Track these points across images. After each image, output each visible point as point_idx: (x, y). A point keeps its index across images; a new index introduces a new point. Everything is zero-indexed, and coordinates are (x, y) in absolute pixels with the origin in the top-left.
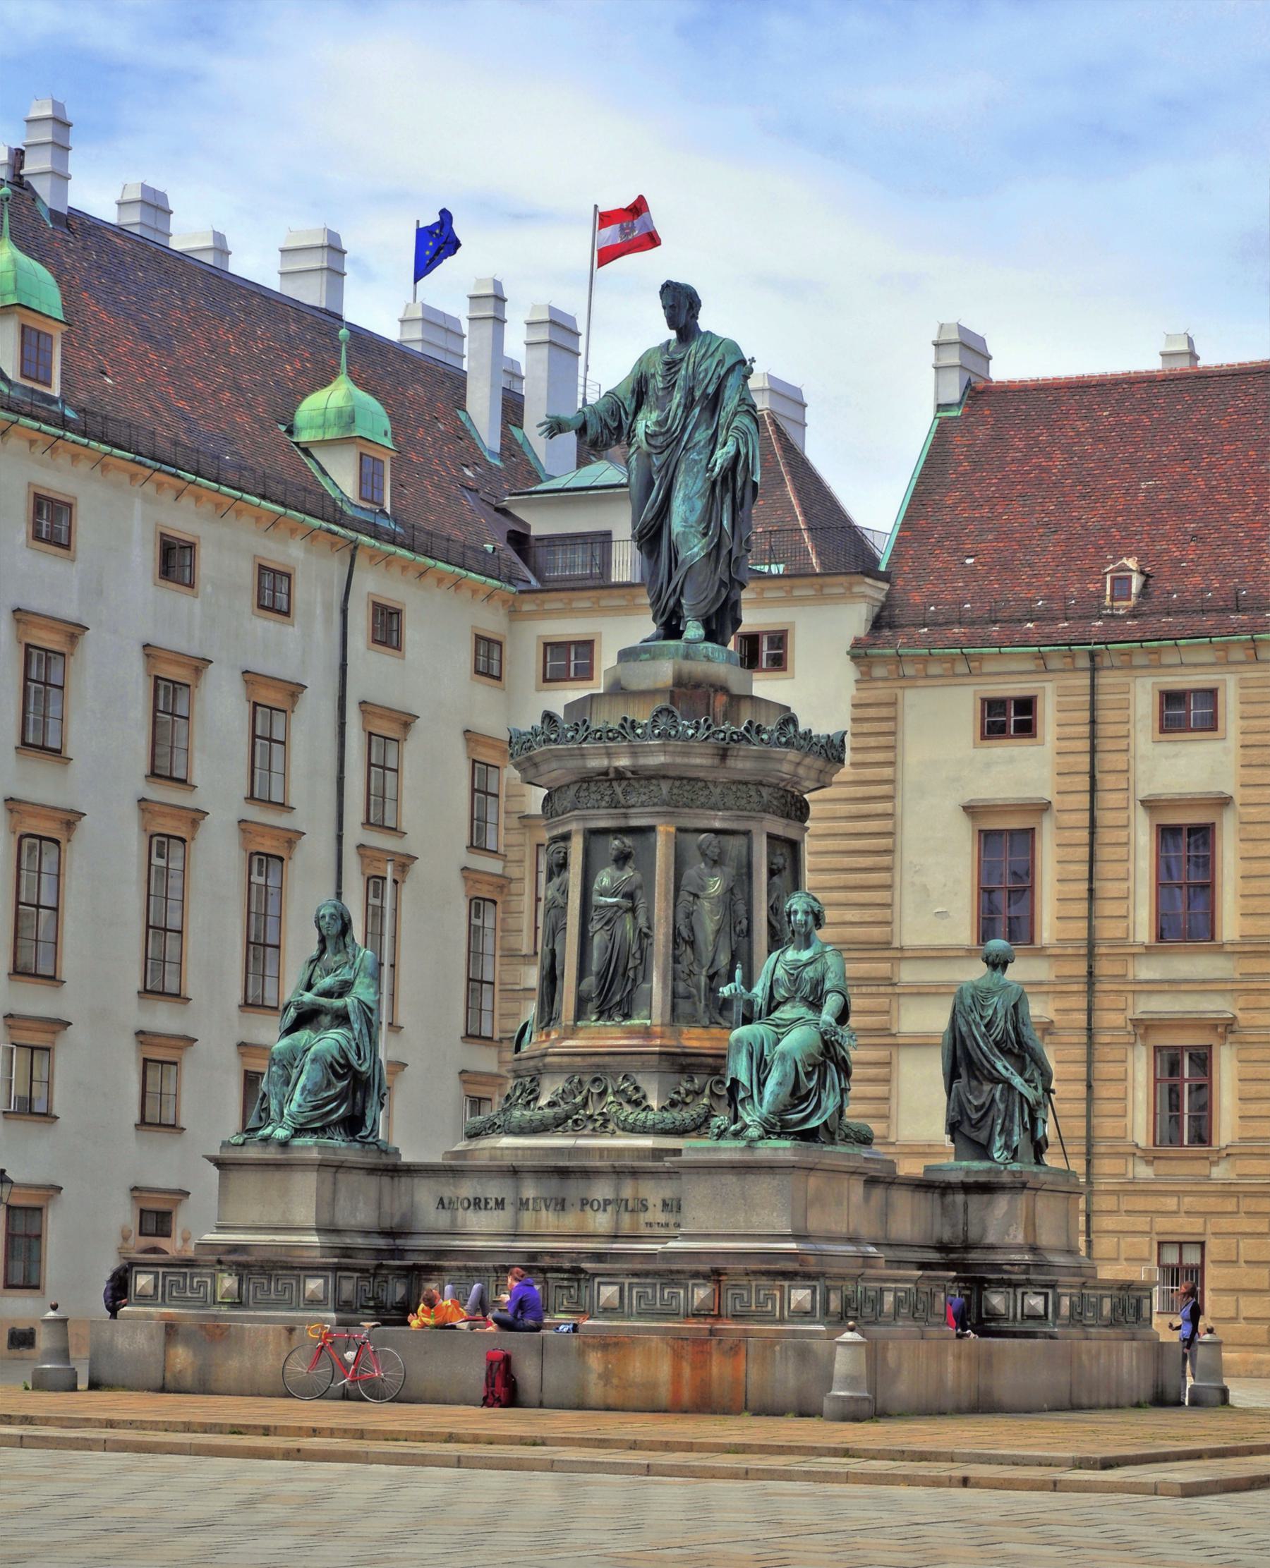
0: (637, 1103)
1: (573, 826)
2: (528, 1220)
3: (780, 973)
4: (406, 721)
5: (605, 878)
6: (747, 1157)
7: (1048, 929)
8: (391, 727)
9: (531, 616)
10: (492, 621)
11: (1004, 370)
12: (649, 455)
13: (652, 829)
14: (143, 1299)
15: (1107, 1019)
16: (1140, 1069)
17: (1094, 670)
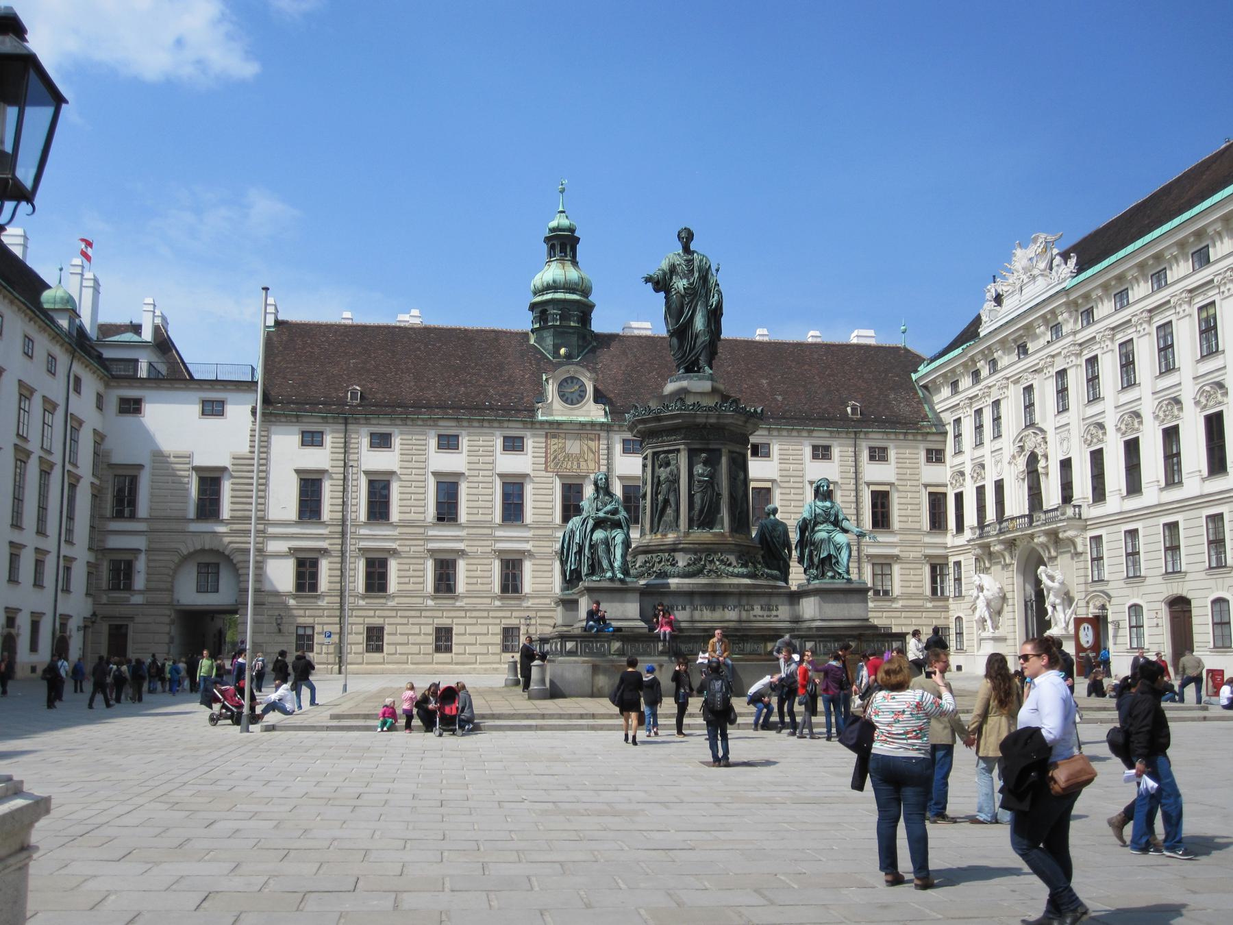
0: (730, 565)
1: (682, 447)
2: (697, 615)
3: (818, 511)
4: (81, 423)
5: (699, 469)
6: (847, 586)
7: (326, 515)
8: (74, 425)
9: (114, 387)
10: (101, 389)
11: (281, 317)
12: (683, 296)
13: (719, 450)
14: (571, 653)
15: (351, 547)
16: (361, 565)
17: (346, 424)
